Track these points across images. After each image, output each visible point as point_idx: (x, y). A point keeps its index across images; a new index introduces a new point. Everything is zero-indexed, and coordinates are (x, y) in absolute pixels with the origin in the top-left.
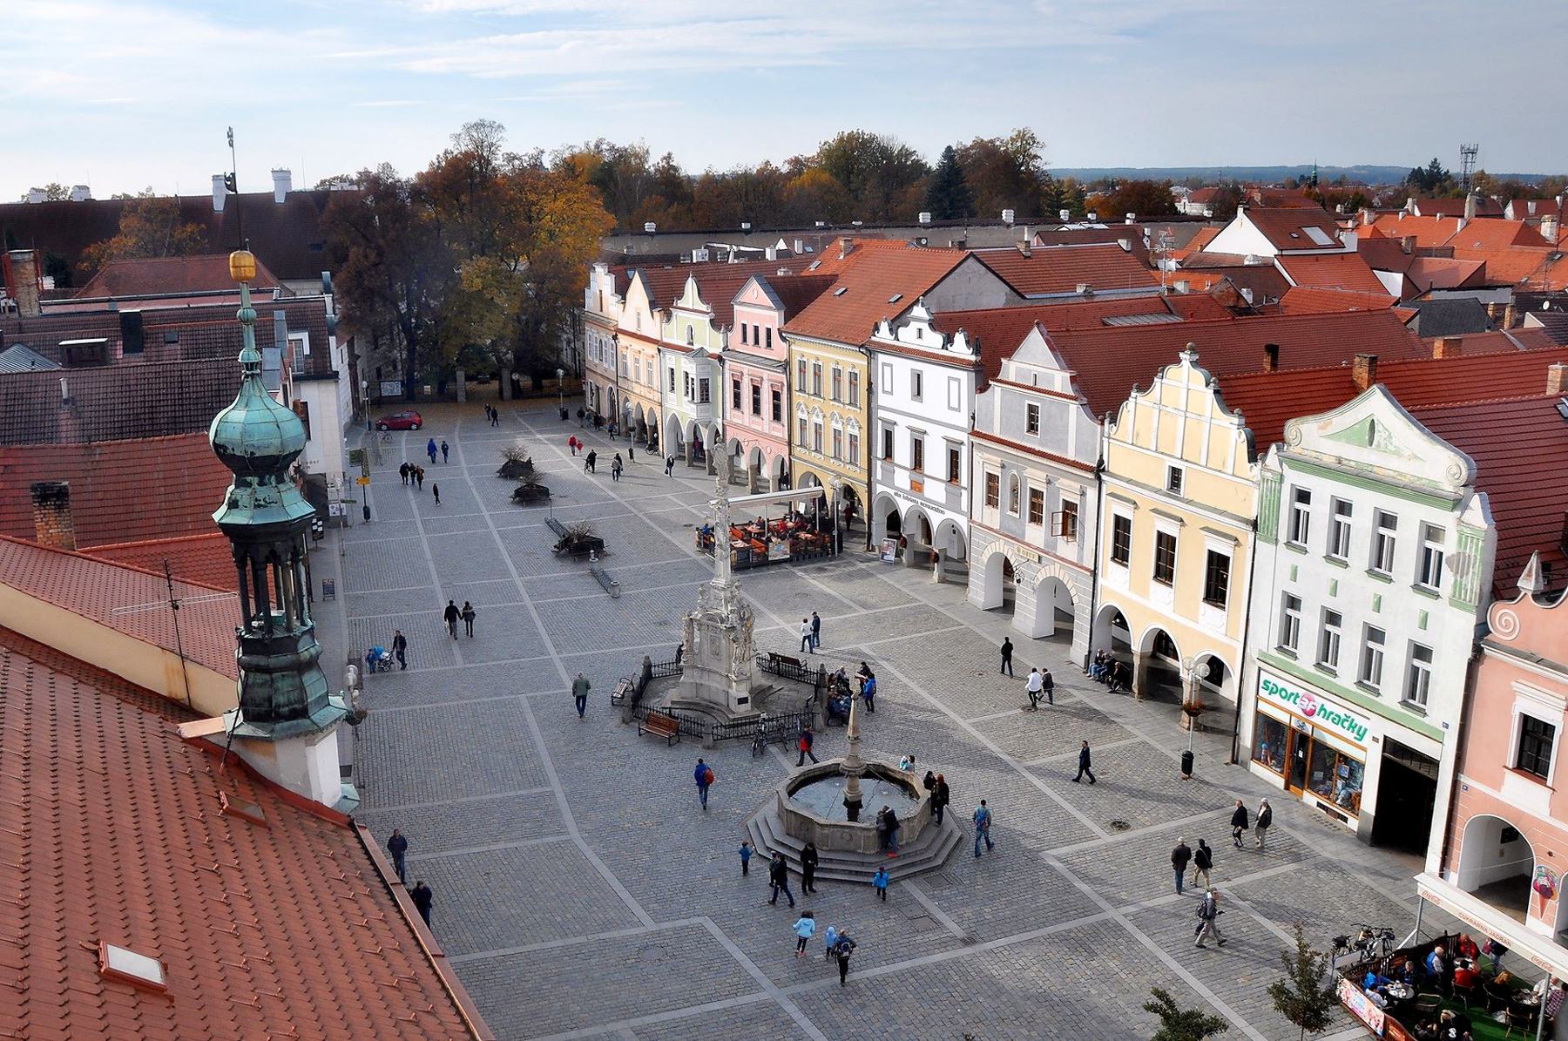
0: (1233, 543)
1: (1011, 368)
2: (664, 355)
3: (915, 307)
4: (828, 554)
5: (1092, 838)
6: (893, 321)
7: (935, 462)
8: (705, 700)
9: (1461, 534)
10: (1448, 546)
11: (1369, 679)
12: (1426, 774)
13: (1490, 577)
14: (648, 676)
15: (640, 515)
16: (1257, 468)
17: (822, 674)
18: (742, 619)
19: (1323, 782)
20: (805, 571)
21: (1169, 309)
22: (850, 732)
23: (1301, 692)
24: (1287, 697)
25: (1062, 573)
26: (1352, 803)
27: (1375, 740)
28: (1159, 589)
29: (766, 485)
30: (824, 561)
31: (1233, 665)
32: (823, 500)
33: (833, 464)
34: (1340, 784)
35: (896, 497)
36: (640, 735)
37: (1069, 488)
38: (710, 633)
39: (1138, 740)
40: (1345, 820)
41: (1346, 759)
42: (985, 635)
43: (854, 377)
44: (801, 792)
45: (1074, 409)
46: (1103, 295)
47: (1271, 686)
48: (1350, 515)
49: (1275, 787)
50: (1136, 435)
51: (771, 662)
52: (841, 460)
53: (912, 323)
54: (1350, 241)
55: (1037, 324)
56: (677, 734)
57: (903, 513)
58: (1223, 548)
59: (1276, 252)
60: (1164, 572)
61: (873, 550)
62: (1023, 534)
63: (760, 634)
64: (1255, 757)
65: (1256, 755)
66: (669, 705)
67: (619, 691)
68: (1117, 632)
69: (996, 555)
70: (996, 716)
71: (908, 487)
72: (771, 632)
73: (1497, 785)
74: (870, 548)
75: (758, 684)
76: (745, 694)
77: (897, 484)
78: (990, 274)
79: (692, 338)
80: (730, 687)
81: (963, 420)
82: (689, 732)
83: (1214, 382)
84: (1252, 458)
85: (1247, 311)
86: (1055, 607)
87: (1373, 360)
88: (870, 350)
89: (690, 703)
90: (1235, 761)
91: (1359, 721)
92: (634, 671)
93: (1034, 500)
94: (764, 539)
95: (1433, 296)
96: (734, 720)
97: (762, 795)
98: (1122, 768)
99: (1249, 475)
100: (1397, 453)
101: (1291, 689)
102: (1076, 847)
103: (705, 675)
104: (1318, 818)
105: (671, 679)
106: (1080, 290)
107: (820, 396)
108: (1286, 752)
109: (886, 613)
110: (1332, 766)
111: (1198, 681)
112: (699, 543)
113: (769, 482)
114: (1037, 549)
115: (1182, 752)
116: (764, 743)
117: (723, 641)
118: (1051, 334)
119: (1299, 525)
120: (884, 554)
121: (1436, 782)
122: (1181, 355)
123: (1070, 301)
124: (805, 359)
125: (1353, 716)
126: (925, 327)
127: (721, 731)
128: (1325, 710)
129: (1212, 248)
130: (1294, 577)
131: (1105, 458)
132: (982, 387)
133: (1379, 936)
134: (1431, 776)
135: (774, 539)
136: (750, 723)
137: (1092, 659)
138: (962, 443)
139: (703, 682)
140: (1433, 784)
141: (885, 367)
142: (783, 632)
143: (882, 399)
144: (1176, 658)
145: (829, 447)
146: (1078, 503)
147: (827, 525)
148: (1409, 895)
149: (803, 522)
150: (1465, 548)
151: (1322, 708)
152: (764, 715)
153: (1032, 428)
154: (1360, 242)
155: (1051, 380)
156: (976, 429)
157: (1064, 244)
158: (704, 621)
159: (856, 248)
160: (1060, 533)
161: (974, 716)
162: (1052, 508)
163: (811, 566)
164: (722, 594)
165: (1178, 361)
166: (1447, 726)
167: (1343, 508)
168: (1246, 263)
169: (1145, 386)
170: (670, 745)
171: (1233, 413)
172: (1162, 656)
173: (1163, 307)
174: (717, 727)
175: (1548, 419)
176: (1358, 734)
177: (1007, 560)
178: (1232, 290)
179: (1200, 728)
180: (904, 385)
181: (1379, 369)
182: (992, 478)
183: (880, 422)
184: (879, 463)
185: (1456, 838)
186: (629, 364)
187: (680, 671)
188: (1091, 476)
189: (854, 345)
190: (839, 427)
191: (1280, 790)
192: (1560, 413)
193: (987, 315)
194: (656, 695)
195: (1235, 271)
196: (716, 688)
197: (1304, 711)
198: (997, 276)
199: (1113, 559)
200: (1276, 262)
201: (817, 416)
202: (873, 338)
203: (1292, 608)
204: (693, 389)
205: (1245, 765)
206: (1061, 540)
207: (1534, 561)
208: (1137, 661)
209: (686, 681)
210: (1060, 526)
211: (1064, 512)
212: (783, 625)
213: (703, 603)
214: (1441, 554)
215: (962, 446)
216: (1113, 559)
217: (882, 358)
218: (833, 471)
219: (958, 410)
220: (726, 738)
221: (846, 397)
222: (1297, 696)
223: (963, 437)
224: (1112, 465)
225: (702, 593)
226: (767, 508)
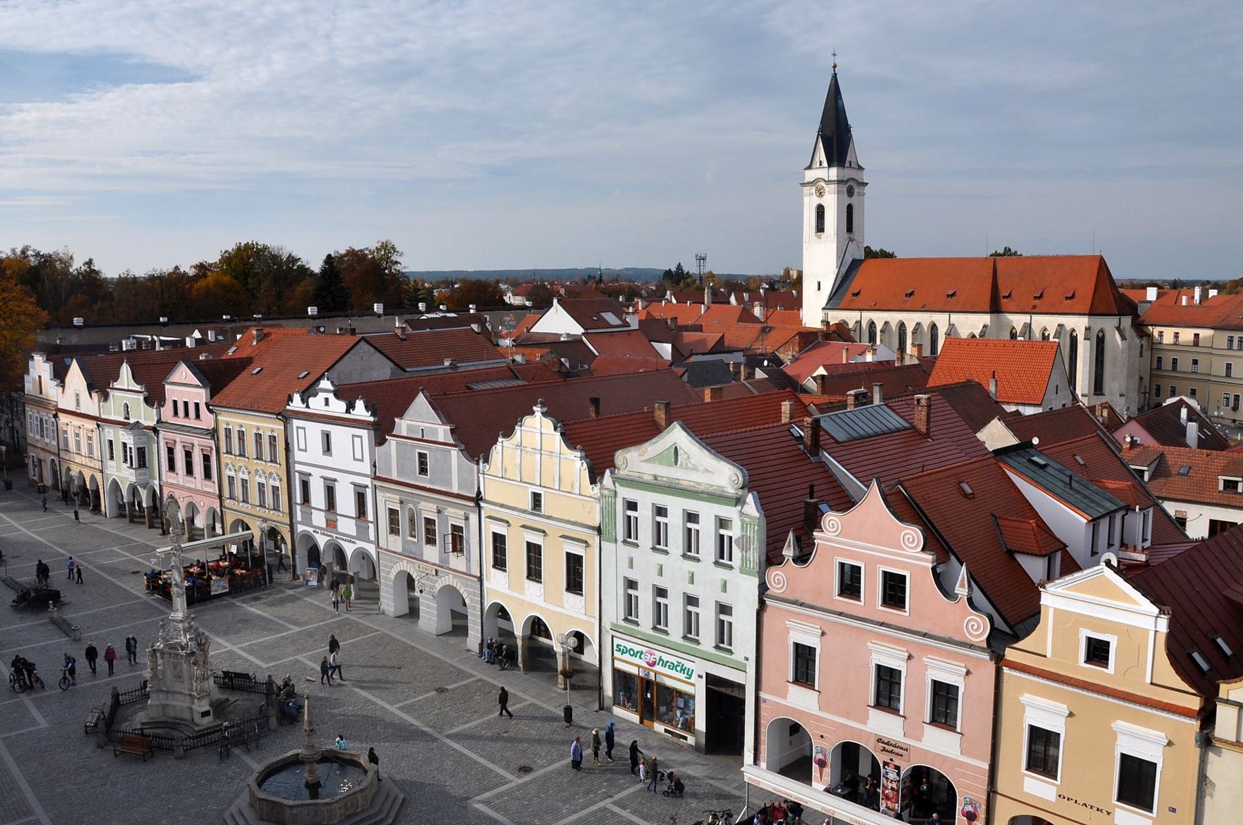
0: (584, 545)
1: (403, 425)
2: (103, 429)
3: (322, 381)
4: (261, 585)
5: (506, 783)
6: (304, 392)
7: (346, 502)
8: (172, 718)
9: (743, 522)
10: (735, 532)
11: (691, 633)
12: (737, 696)
13: (764, 550)
14: (116, 704)
15: (91, 567)
16: (597, 489)
17: (270, 683)
18: (199, 645)
19: (667, 713)
20: (244, 602)
21: (515, 375)
22: (306, 727)
23: (644, 650)
24: (635, 655)
25: (455, 583)
26: (689, 726)
27: (700, 676)
28: (532, 586)
29: (201, 532)
30: (259, 591)
31: (592, 636)
32: (251, 541)
33: (259, 511)
34: (678, 713)
35: (314, 534)
36: (116, 756)
37: (454, 515)
38: (172, 660)
39: (528, 703)
40: (685, 738)
41: (680, 694)
42: (398, 637)
43: (273, 439)
44: (268, 782)
45: (455, 453)
46: (464, 367)
47: (622, 648)
48: (666, 516)
49: (633, 723)
50: (505, 470)
51: (224, 678)
52: (265, 507)
53: (320, 394)
54: (634, 322)
55: (422, 390)
56: (150, 750)
57: (321, 546)
58: (577, 550)
59: (583, 331)
60: (534, 573)
61: (298, 578)
62: (422, 555)
63: (212, 656)
64: (616, 702)
65: (617, 701)
66: (139, 727)
67: (91, 720)
68: (502, 623)
69: (401, 572)
70: (416, 699)
71: (324, 526)
72: (220, 654)
73: (784, 696)
74: (295, 577)
75: (216, 698)
76: (207, 708)
78: (378, 354)
79: (128, 414)
80: (193, 703)
81: (366, 468)
82: (160, 748)
83: (560, 427)
84: (593, 481)
85: (566, 375)
86: (452, 610)
87: (667, 405)
88: (286, 417)
89: (159, 722)
90: (601, 708)
91: (687, 665)
92: (103, 701)
93: (428, 527)
94: (205, 577)
95: (694, 359)
96: (200, 731)
97: (233, 791)
98: (520, 726)
99: (591, 493)
100: (695, 469)
101: (637, 648)
102: (495, 792)
104: (666, 740)
105: (140, 703)
106: (447, 363)
107: (244, 456)
108: (637, 696)
109: (315, 628)
110: (672, 701)
111: (569, 651)
112: (148, 587)
113: (203, 530)
114: (434, 564)
115: (562, 707)
116: (229, 746)
117: (185, 666)
118: (435, 397)
119: (631, 528)
120: (308, 581)
121: (744, 700)
122: (534, 408)
123: (441, 372)
124: (230, 427)
125: (683, 661)
126: (331, 396)
127: (189, 742)
128: (663, 661)
129: (537, 329)
130: (631, 567)
131: (482, 490)
132: (380, 441)
133: (722, 817)
134: (740, 697)
135: (214, 578)
136: (214, 732)
137: (485, 645)
138: (367, 486)
139: (168, 702)
140: (743, 702)
141: (299, 430)
142: (231, 653)
143: (298, 456)
144: (548, 636)
146: (463, 525)
147: (258, 561)
148: (736, 785)
149: (236, 560)
150: (746, 532)
152: (226, 724)
153: (423, 470)
154: (641, 322)
155: (435, 432)
156: (377, 475)
157: (431, 328)
158: (167, 650)
159: (267, 335)
160: (451, 550)
161: (399, 701)
162: (443, 531)
163: (248, 596)
164: (181, 625)
165: (532, 413)
166: (747, 659)
167: (661, 511)
168: (562, 339)
169: (508, 433)
170: (145, 761)
171: (576, 448)
172: (536, 637)
173: (511, 373)
174: (186, 739)
175: (785, 439)
176: (687, 674)
178: (556, 359)
179: (573, 687)
180: (316, 443)
181: (672, 411)
182: (393, 513)
183: (297, 474)
184: (298, 508)
185: (762, 738)
186: (70, 439)
187: (147, 696)
188: (472, 504)
189: (271, 413)
190: (263, 480)
191: (637, 725)
192: (792, 435)
193: (379, 385)
194: (126, 720)
195: (552, 343)
196: (181, 706)
197: (648, 663)
198: (383, 354)
199: (494, 566)
200: (584, 338)
201: (243, 472)
202: (288, 407)
203: (631, 588)
204: (131, 457)
205: (609, 710)
207: (791, 536)
208: (519, 643)
209: (154, 703)
210: (451, 545)
211: (452, 534)
212: (230, 647)
213: (164, 635)
214: (731, 538)
215: (367, 489)
216: (494, 566)
217: (296, 423)
218: (259, 517)
219: (362, 460)
220: (195, 748)
221: (267, 454)
222: (642, 653)
223: (367, 481)
224: (488, 494)
225: (162, 626)
226: (202, 553)
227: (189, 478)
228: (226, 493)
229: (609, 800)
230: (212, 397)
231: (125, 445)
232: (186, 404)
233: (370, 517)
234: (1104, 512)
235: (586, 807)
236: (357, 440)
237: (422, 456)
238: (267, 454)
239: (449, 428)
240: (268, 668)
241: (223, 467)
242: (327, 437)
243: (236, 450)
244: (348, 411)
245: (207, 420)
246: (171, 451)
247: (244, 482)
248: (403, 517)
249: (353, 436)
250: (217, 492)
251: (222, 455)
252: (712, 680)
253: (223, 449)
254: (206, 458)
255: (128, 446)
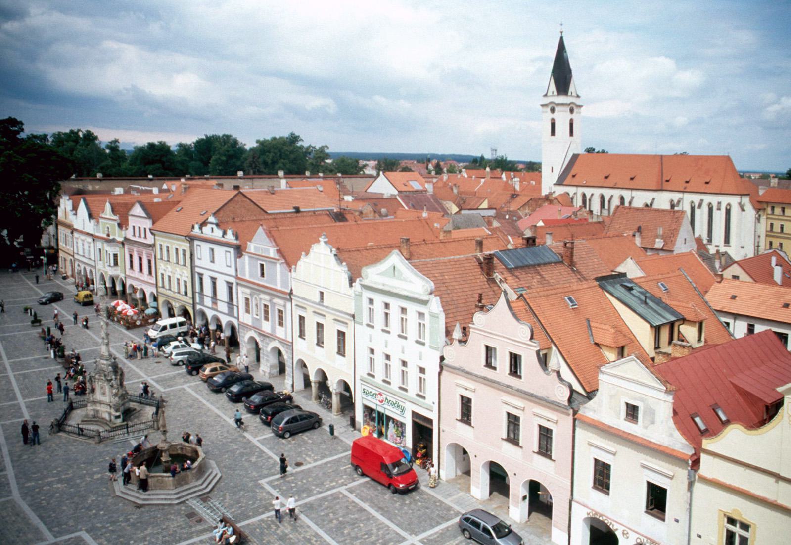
1: (252, 247)
16: (351, 292)
43: (184, 251)
47: (366, 391)
55: (262, 225)
57: (209, 318)
60: (320, 342)
77: (206, 304)
84: (351, 285)
88: (191, 239)
91: (401, 404)
103: (98, 405)
138: (232, 283)
145: (175, 287)
151: (386, 399)
153: (263, 275)
155: (268, 251)
177: (256, 341)
202: (192, 233)
206: (278, 327)
208: (313, 384)
217: (196, 242)
219: (230, 267)
223: (232, 280)
227: (141, 274)
228: (160, 284)
229: (345, 487)
230: (154, 223)
231: (107, 251)
232: (140, 228)
233: (235, 302)
234: (665, 321)
235: (328, 489)
236: (228, 254)
237: (262, 266)
238: (181, 262)
239: (275, 249)
240: (164, 392)
241: (158, 267)
242: (212, 250)
243: (165, 258)
244: (223, 236)
245: (150, 240)
246: (131, 256)
247: (169, 277)
248: (252, 302)
249: (226, 252)
250: (155, 283)
251: (157, 260)
252: (414, 414)
253: (158, 257)
254: (150, 262)
255: (108, 252)
